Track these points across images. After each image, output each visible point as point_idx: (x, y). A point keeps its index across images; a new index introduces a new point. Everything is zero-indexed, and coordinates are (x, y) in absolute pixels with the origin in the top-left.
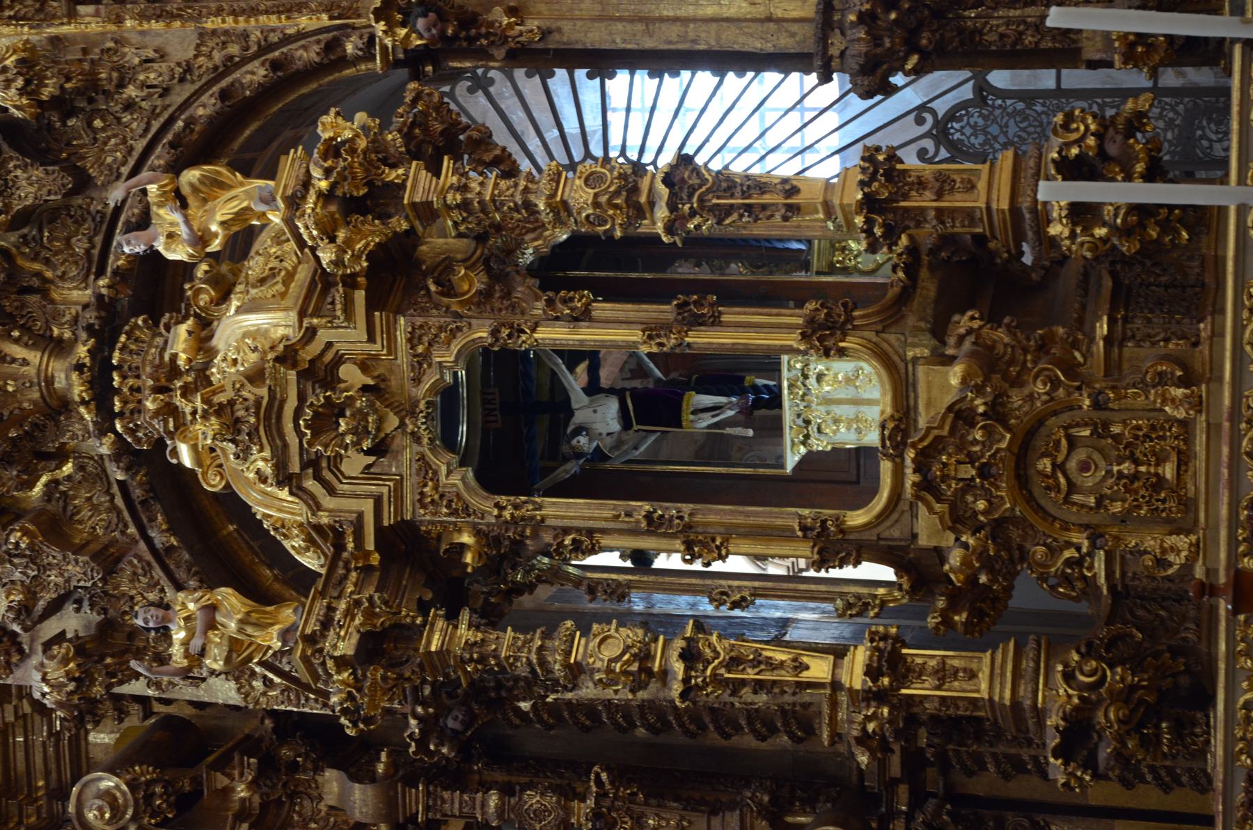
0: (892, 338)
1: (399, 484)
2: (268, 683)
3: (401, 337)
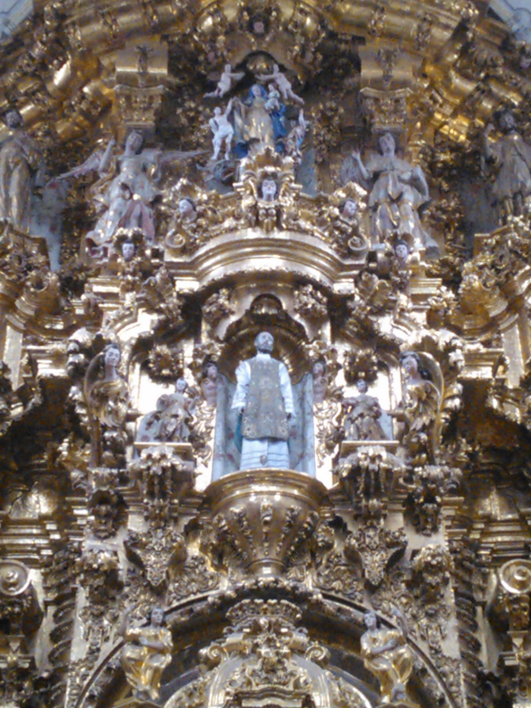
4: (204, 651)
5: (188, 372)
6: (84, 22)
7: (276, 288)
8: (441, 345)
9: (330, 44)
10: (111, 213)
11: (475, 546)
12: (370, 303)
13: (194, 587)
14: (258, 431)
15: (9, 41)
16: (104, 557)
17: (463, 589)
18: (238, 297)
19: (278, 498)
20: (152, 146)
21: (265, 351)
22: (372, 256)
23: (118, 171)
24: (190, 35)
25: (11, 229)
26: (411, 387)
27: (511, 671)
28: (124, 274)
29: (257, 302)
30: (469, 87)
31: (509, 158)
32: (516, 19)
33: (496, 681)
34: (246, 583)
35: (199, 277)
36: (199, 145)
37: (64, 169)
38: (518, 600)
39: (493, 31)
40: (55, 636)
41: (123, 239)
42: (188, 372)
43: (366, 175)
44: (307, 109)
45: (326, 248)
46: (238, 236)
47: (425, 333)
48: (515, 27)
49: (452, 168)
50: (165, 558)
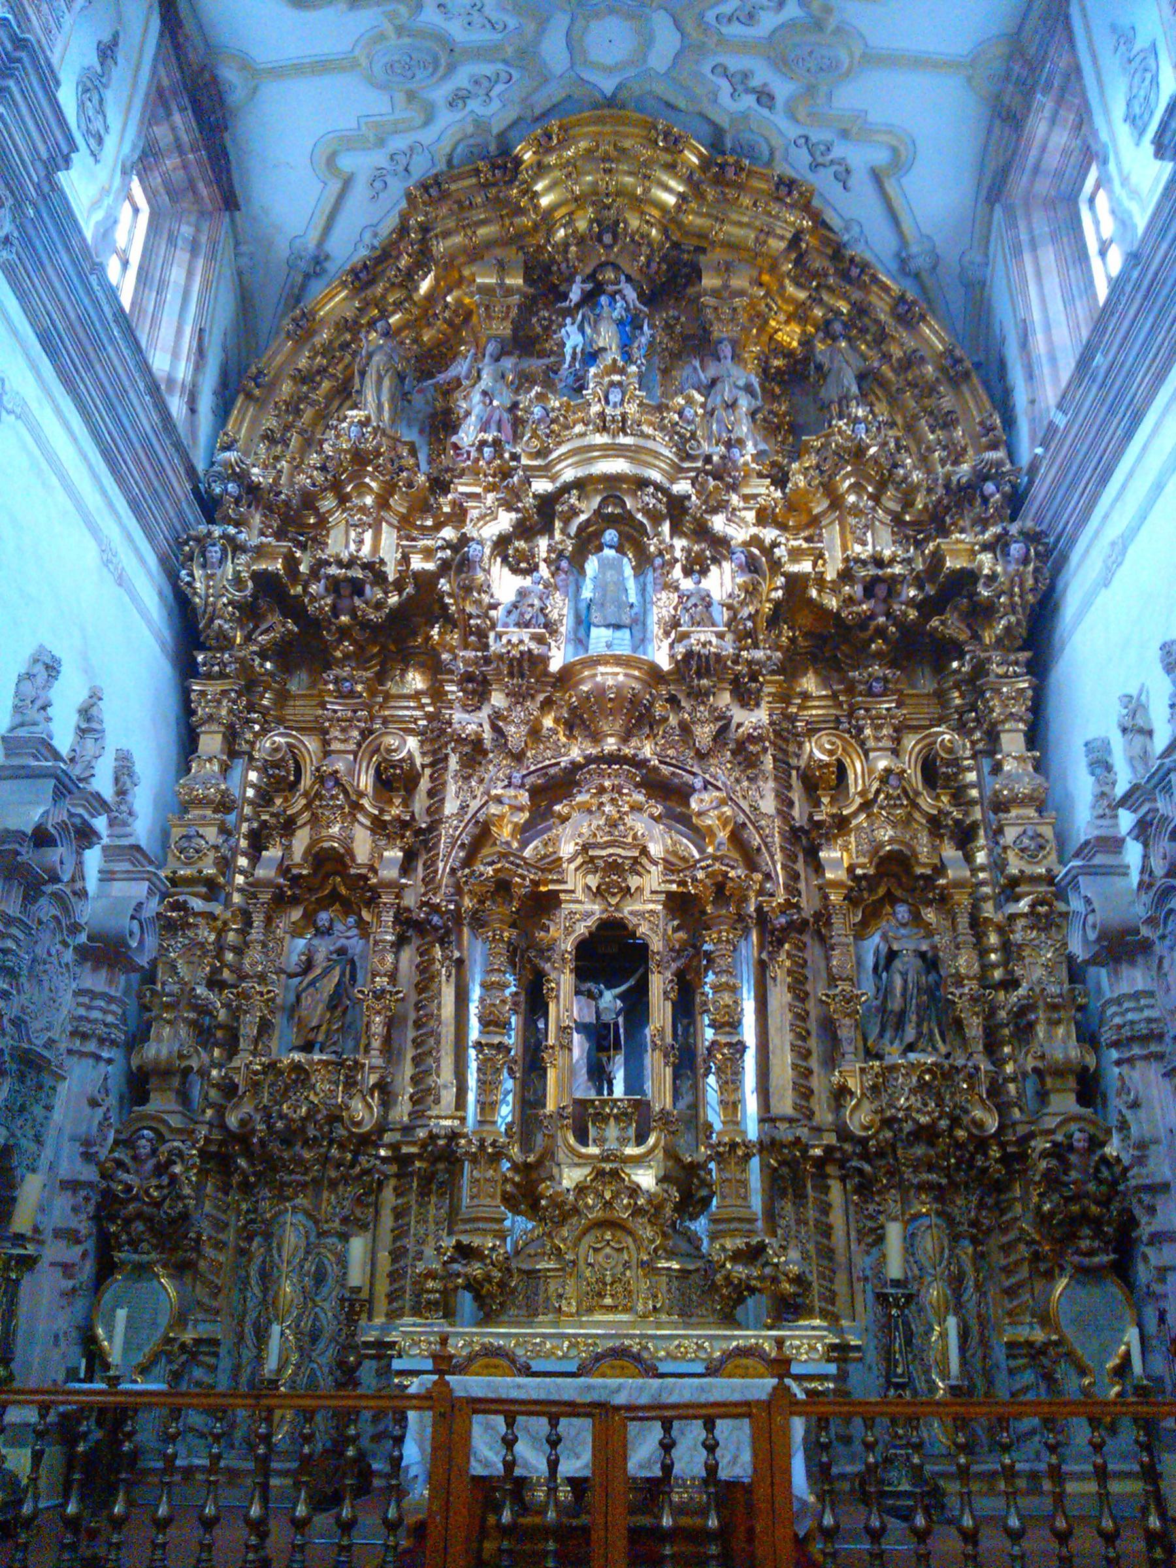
0: (661, 1155)
1: (580, 902)
2: (456, 828)
3: (651, 906)
4: (557, 808)
5: (543, 566)
6: (446, 234)
7: (620, 489)
8: (767, 542)
10: (473, 418)
11: (792, 719)
12: (705, 502)
13: (549, 753)
14: (605, 618)
15: (378, 253)
17: (780, 756)
18: (587, 498)
19: (621, 678)
20: (510, 354)
21: (611, 547)
22: (708, 459)
23: (479, 378)
25: (384, 434)
26: (740, 580)
27: (819, 825)
28: (485, 476)
29: (604, 503)
30: (802, 295)
31: (836, 364)
32: (847, 229)
33: (806, 833)
34: (593, 751)
35: (553, 479)
36: (552, 352)
37: (431, 375)
38: (827, 765)
39: (826, 241)
40: (431, 794)
41: (483, 443)
42: (543, 566)
43: (705, 381)
44: (650, 317)
45: (666, 452)
46: (587, 441)
47: (754, 530)
48: (846, 238)
49: (784, 373)
50: (524, 729)
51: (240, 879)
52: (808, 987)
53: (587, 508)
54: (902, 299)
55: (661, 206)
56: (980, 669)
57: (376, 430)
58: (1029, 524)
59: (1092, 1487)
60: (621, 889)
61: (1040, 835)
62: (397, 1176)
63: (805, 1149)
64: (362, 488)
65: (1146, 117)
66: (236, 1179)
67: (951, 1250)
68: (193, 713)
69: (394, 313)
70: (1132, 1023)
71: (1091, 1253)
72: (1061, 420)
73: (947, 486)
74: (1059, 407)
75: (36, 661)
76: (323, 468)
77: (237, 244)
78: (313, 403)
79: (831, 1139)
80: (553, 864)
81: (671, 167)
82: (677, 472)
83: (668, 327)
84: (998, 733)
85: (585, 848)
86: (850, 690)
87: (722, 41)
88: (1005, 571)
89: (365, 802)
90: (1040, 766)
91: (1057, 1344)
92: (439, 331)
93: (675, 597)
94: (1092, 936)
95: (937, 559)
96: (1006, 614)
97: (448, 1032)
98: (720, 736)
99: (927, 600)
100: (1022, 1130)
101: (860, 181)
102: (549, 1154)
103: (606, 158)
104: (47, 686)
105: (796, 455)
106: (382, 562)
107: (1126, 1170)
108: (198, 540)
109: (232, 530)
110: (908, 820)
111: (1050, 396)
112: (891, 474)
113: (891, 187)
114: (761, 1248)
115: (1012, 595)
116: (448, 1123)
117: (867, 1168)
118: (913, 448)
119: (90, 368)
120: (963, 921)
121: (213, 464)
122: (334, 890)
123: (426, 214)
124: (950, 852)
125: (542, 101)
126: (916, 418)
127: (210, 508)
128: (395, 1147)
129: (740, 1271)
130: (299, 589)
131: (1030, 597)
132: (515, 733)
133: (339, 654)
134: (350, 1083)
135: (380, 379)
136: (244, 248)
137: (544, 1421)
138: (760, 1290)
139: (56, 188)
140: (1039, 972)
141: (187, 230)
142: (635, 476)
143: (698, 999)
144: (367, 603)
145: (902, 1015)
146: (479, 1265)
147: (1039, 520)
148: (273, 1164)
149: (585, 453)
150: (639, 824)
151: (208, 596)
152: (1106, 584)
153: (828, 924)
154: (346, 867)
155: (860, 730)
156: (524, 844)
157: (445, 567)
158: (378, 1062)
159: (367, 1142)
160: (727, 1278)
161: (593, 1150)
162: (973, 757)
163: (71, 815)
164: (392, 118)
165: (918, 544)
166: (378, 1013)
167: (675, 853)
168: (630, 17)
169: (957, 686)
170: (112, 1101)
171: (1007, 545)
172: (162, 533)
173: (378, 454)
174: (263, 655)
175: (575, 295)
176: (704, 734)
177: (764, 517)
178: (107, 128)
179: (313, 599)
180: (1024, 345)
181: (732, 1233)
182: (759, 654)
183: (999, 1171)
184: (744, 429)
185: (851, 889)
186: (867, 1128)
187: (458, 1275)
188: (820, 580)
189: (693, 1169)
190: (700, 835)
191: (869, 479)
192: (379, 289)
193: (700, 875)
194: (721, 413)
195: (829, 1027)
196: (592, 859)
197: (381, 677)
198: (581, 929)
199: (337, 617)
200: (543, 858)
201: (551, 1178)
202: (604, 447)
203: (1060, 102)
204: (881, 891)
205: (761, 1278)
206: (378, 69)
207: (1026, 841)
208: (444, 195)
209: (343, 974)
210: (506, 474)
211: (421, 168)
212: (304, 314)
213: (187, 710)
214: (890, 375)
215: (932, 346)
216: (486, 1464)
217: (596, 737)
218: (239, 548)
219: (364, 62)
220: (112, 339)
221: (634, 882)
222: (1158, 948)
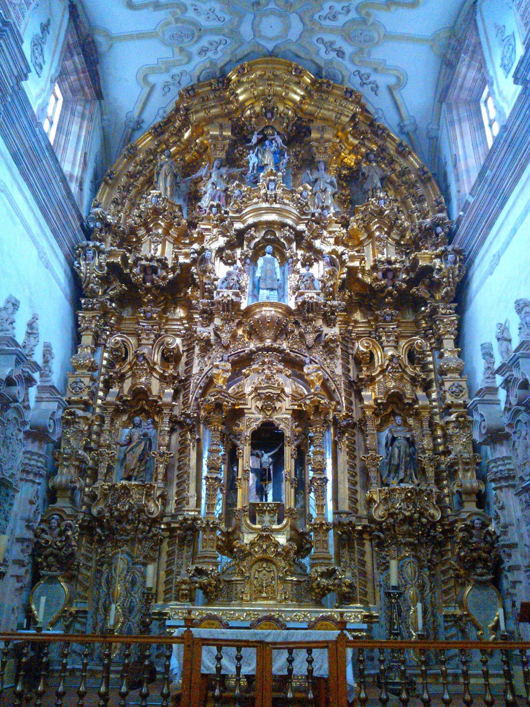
0: (289, 529)
1: (253, 414)
2: (198, 379)
3: (286, 416)
4: (244, 371)
6: (197, 112)
7: (274, 227)
8: (340, 252)
9: (299, 122)
10: (207, 195)
11: (350, 332)
12: (312, 234)
13: (240, 346)
15: (166, 120)
16: (205, 334)
17: (344, 349)
18: (259, 231)
19: (273, 313)
20: (225, 166)
21: (269, 253)
22: (313, 215)
23: (211, 177)
24: (241, 118)
25: (167, 201)
26: (327, 269)
27: (362, 380)
28: (213, 221)
30: (356, 142)
31: (371, 174)
32: (377, 113)
33: (355, 383)
34: (261, 346)
35: (243, 223)
36: (244, 166)
37: (189, 175)
38: (365, 353)
39: (367, 118)
40: (187, 364)
41: (212, 206)
43: (312, 180)
44: (288, 151)
45: (294, 211)
46: (259, 206)
47: (334, 247)
50: (229, 335)
51: (99, 402)
52: (356, 453)
53: (259, 236)
54: (400, 145)
55: (293, 101)
56: (434, 311)
57: (164, 199)
58: (457, 246)
59: (482, 681)
60: (272, 408)
61: (460, 386)
62: (170, 537)
63: (354, 527)
64: (157, 226)
65: (510, 64)
66: (96, 538)
67: (420, 572)
68: (79, 326)
69: (172, 147)
70: (501, 471)
71: (481, 575)
72: (471, 200)
73: (420, 228)
74: (470, 194)
75: (8, 302)
76: (140, 216)
77: (102, 114)
78: (136, 187)
79: (365, 522)
80: (241, 396)
81: (298, 84)
82: (299, 220)
83: (296, 156)
84: (442, 340)
85: (256, 389)
86: (376, 320)
87: (321, 27)
88: (446, 267)
89: (157, 367)
90: (460, 355)
91: (466, 616)
92: (193, 155)
93: (298, 276)
94: (484, 431)
95: (415, 261)
96: (446, 286)
97: (193, 472)
98: (317, 339)
99: (411, 279)
100: (452, 519)
101: (383, 92)
102: (238, 528)
103: (269, 79)
104: (13, 313)
105: (353, 214)
106: (166, 259)
107: (498, 537)
108: (82, 248)
109: (98, 244)
110: (402, 378)
111: (466, 189)
112: (395, 223)
113: (395, 93)
114: (334, 571)
115: (449, 278)
116: (193, 513)
117: (382, 535)
118: (405, 212)
119: (35, 169)
120: (426, 424)
121: (90, 213)
122: (142, 406)
123: (188, 103)
124: (420, 393)
125: (241, 52)
126: (406, 198)
127: (88, 233)
128: (168, 524)
129: (324, 582)
130: (128, 270)
131: (457, 279)
132: (225, 337)
133: (146, 300)
134: (148, 495)
135: (166, 176)
136: (105, 117)
137: (234, 649)
138: (333, 591)
139: (21, 89)
140: (460, 448)
141: (79, 108)
142: (280, 222)
143: (306, 458)
144: (159, 277)
145: (398, 467)
146: (205, 578)
147: (461, 244)
148: (113, 531)
149: (258, 211)
150: (280, 379)
151: (87, 273)
152: (491, 274)
153: (365, 425)
154: (147, 396)
155: (380, 337)
156: (229, 387)
157: (194, 261)
158: (161, 485)
159: (156, 521)
160: (318, 585)
161: (258, 526)
162: (431, 350)
163: (23, 372)
164: (173, 59)
165: (407, 254)
166: (162, 463)
167: (296, 392)
168: (280, 16)
169: (424, 318)
170: (40, 502)
171: (446, 255)
172: (67, 245)
173: (165, 210)
174: (111, 300)
175: (254, 140)
176: (310, 338)
177: (337, 242)
178: (44, 62)
179: (134, 275)
180: (455, 166)
181: (320, 565)
182: (335, 303)
183: (441, 537)
184: (329, 202)
185: (376, 409)
186: (382, 517)
187: (196, 582)
188: (363, 270)
189: (303, 535)
190: (308, 384)
191: (385, 225)
192: (166, 136)
193: (308, 402)
194: (319, 194)
195: (365, 471)
196: (259, 394)
197: (165, 311)
198: (254, 426)
199: (145, 283)
200: (237, 393)
201: (239, 539)
202: (266, 209)
203: (472, 58)
204: (389, 410)
205: (334, 585)
206: (167, 37)
207: (454, 389)
208: (196, 95)
209: (146, 445)
210: (222, 220)
211: (186, 82)
212: (132, 147)
213: (77, 325)
214: (395, 178)
215: (413, 166)
216: (208, 668)
217: (262, 339)
218: (101, 252)
219: (160, 33)
220: (45, 157)
221: (278, 405)
222: (514, 438)
